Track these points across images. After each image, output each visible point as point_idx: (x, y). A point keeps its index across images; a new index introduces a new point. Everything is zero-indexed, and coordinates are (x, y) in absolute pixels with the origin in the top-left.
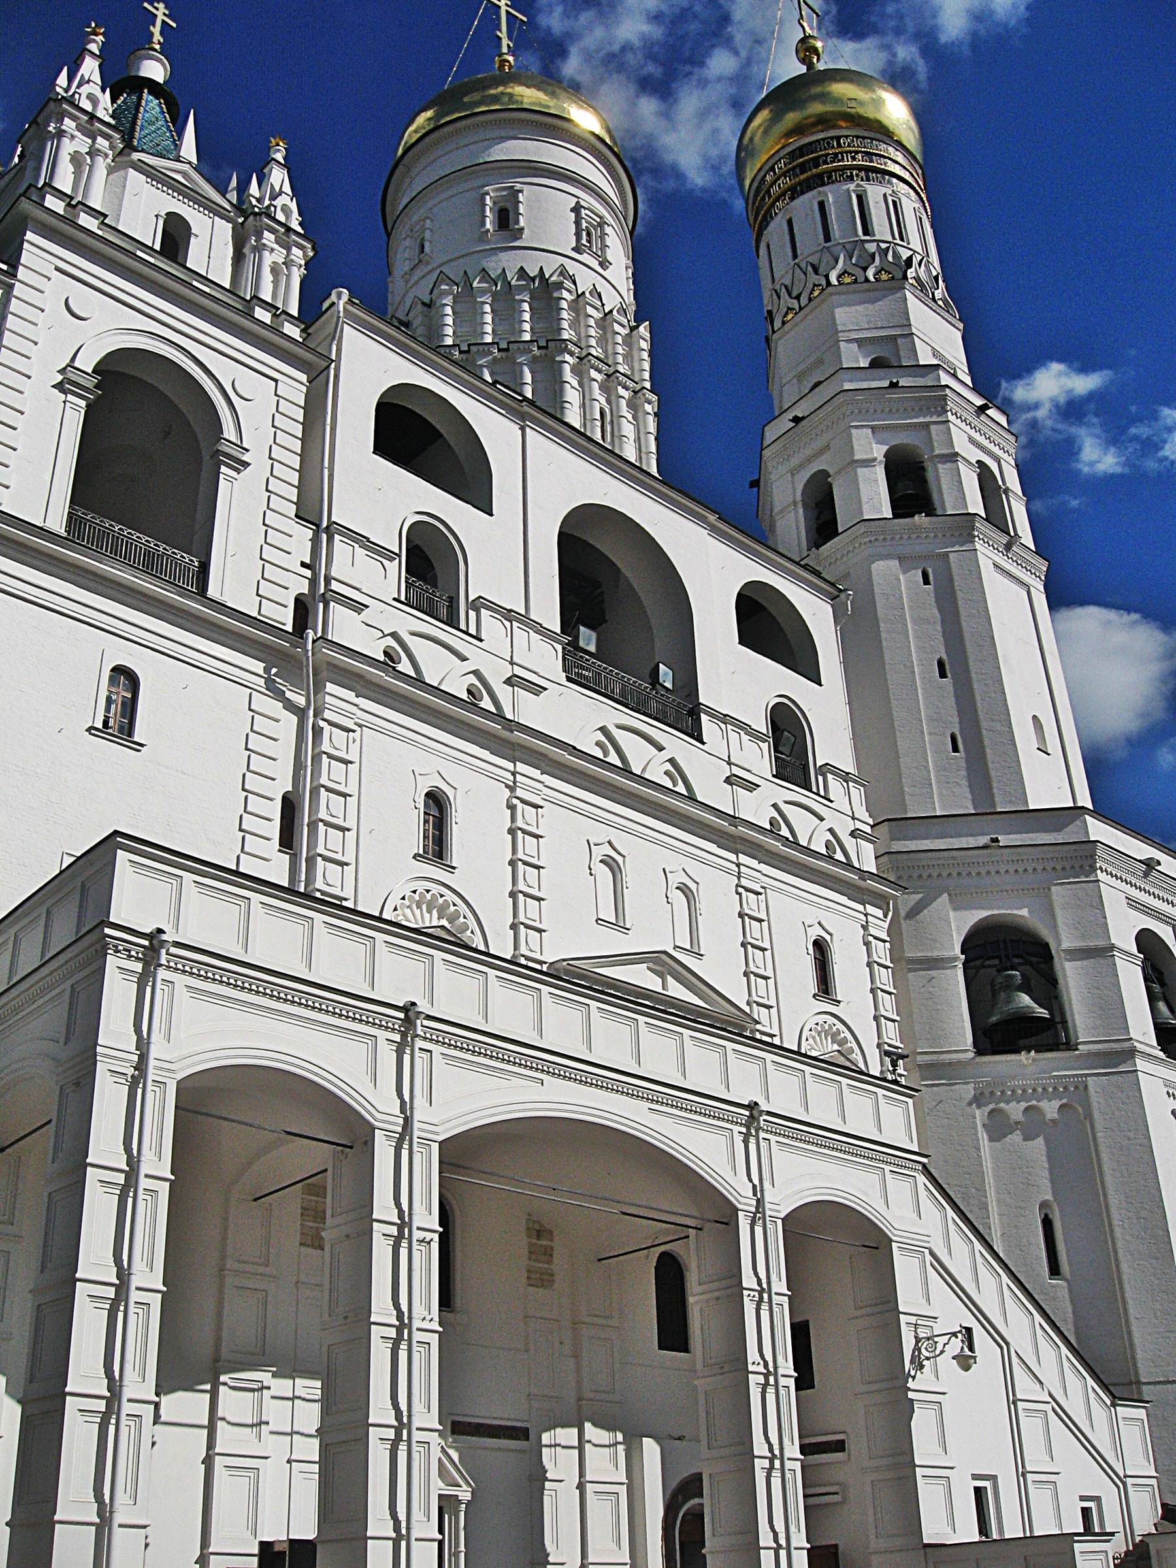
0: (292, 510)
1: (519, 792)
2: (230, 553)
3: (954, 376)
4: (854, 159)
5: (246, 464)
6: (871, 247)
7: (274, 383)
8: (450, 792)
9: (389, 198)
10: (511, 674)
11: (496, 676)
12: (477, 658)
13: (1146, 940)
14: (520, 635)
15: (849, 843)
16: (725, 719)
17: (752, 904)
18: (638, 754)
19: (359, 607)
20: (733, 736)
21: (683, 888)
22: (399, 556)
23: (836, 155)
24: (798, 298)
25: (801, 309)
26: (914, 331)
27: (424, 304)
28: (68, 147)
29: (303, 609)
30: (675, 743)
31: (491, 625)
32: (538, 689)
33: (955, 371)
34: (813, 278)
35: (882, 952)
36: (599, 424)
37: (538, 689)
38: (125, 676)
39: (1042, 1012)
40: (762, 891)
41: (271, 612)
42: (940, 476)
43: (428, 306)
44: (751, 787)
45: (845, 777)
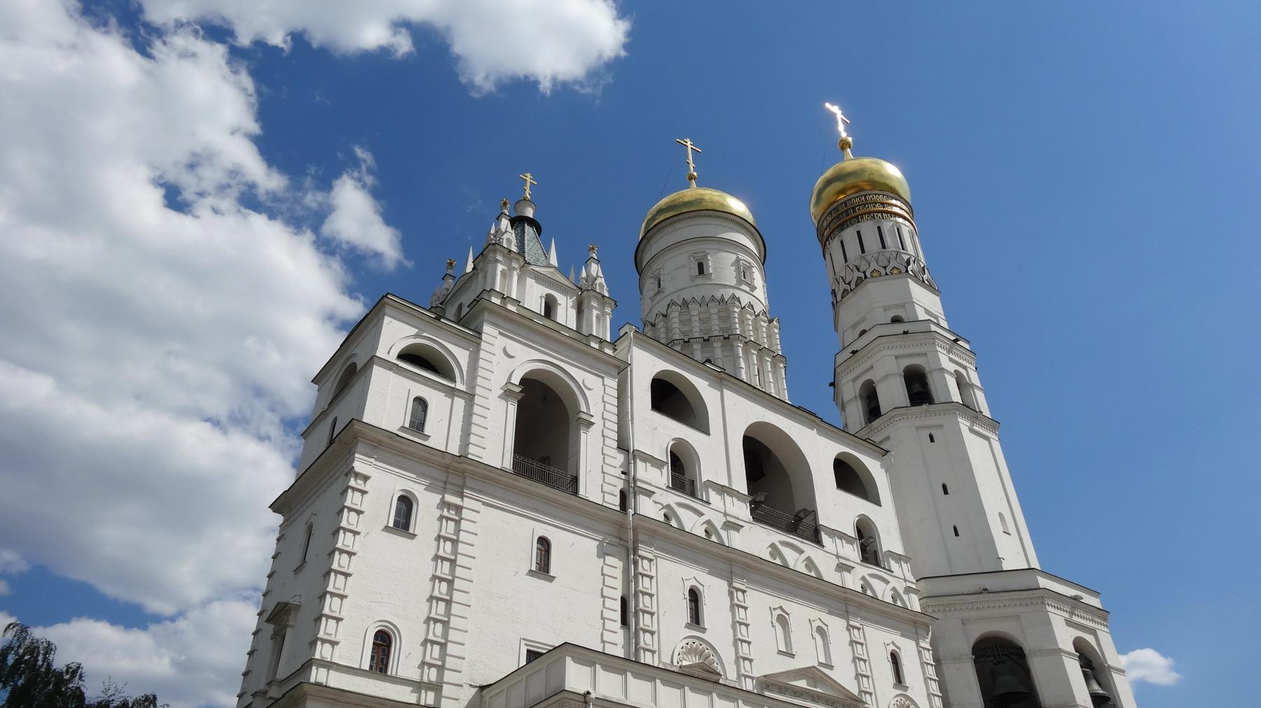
0: (615, 445)
2: (588, 471)
3: (938, 325)
4: (874, 206)
5: (592, 424)
6: (888, 255)
7: (601, 380)
8: (700, 588)
9: (639, 255)
10: (725, 521)
11: (718, 522)
12: (709, 514)
13: (1079, 645)
14: (728, 499)
15: (905, 597)
16: (834, 533)
17: (857, 635)
18: (792, 558)
20: (838, 541)
21: (820, 630)
22: (667, 463)
23: (864, 205)
24: (849, 284)
25: (851, 290)
26: (914, 300)
27: (663, 316)
28: (500, 267)
29: (623, 496)
30: (810, 549)
31: (714, 497)
33: (938, 320)
34: (857, 274)
36: (757, 377)
37: (737, 527)
39: (1021, 689)
40: (861, 627)
41: (609, 498)
42: (933, 382)
43: (665, 316)
45: (898, 558)
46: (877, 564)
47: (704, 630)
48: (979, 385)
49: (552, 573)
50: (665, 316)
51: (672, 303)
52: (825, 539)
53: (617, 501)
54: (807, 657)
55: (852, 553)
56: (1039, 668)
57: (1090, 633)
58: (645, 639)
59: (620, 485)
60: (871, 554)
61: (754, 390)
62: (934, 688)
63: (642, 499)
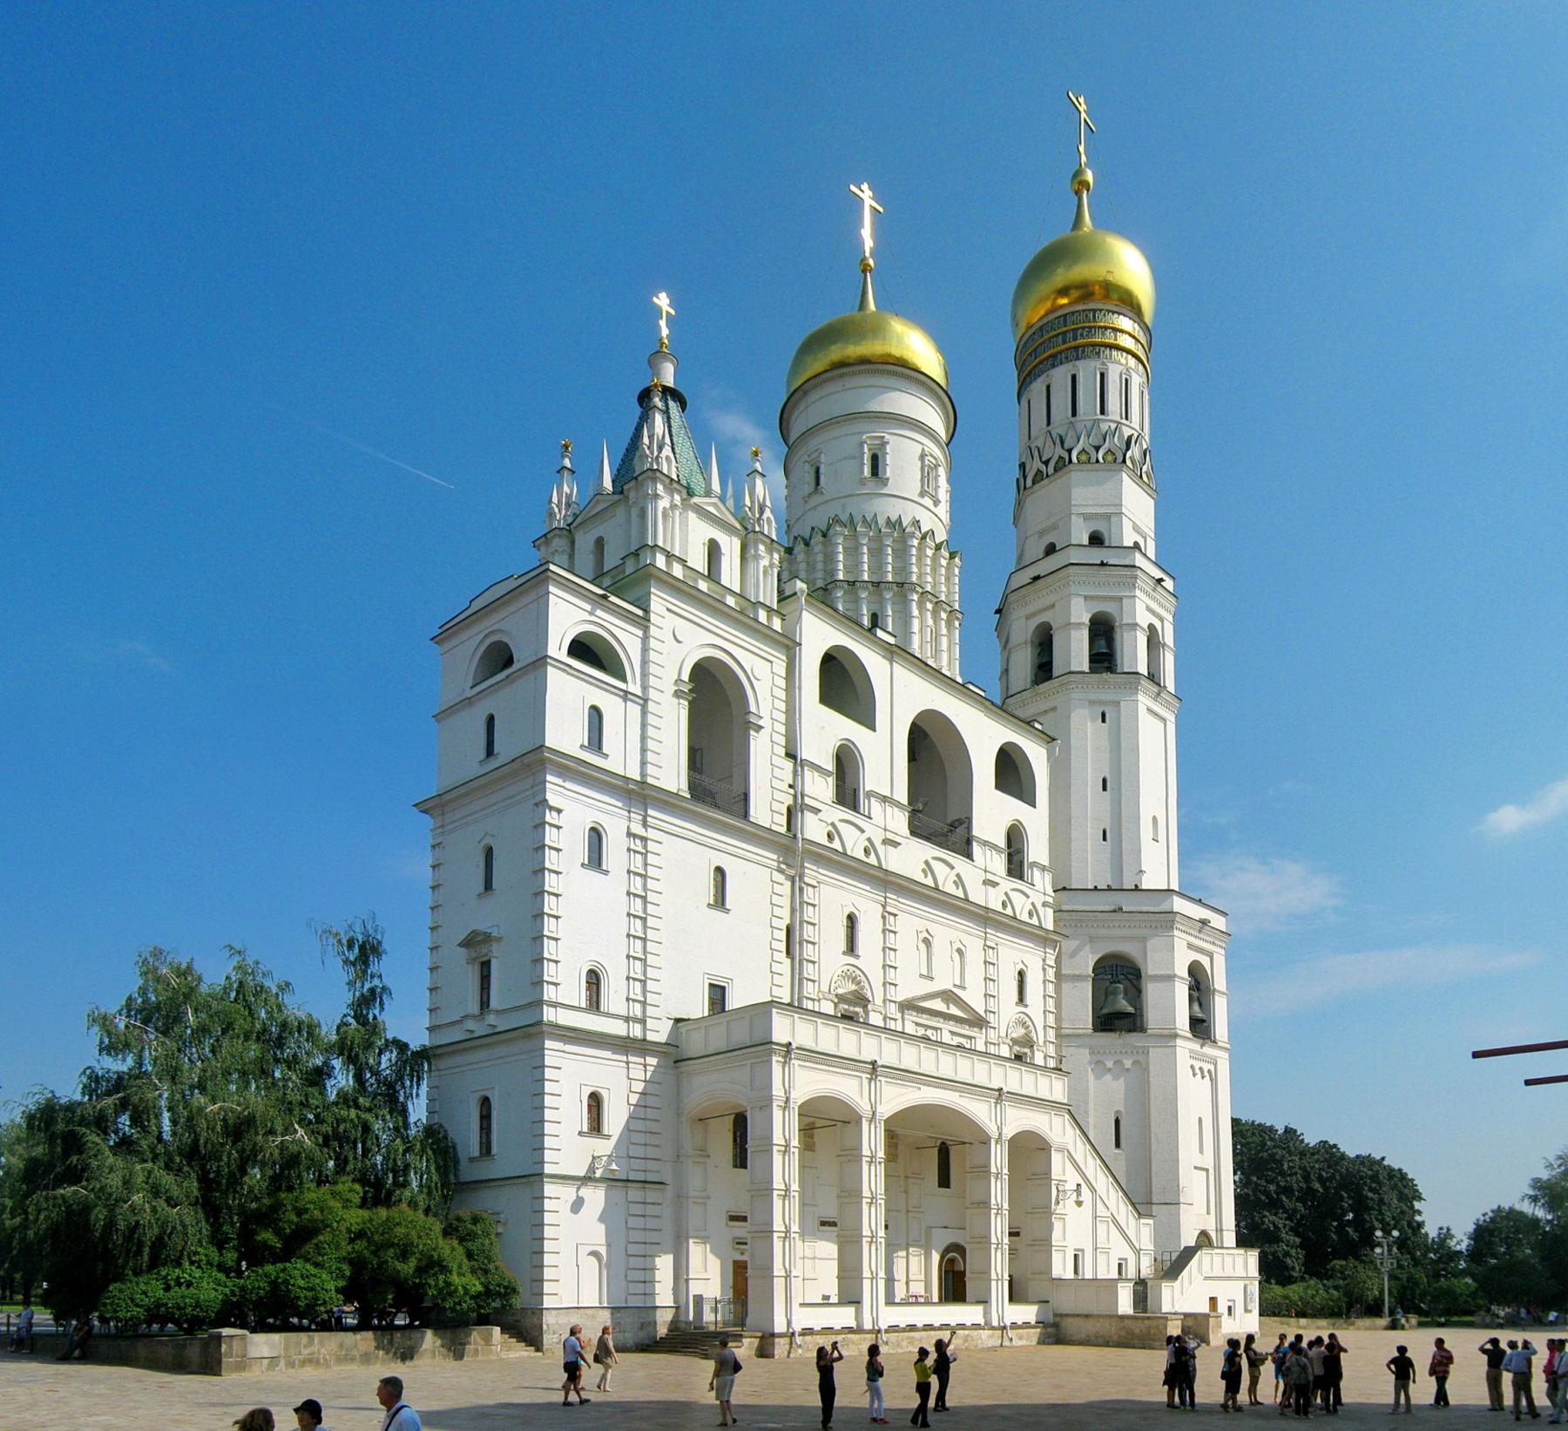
1: (888, 909)
13: (1195, 971)
16: (985, 843)
19: (817, 811)
21: (959, 951)
24: (1046, 463)
25: (1047, 476)
30: (958, 862)
31: (876, 807)
32: (896, 844)
35: (1051, 973)
37: (896, 844)
38: (720, 871)
39: (1131, 1009)
44: (994, 884)
45: (1043, 868)
46: (1021, 878)
47: (857, 957)
48: (1172, 646)
49: (728, 907)
50: (824, 535)
51: (837, 520)
52: (976, 848)
53: (783, 820)
54: (943, 983)
55: (999, 864)
56: (1152, 992)
57: (1207, 955)
58: (809, 970)
59: (789, 801)
60: (1016, 867)
61: (927, 669)
62: (1051, 1002)
63: (808, 815)
